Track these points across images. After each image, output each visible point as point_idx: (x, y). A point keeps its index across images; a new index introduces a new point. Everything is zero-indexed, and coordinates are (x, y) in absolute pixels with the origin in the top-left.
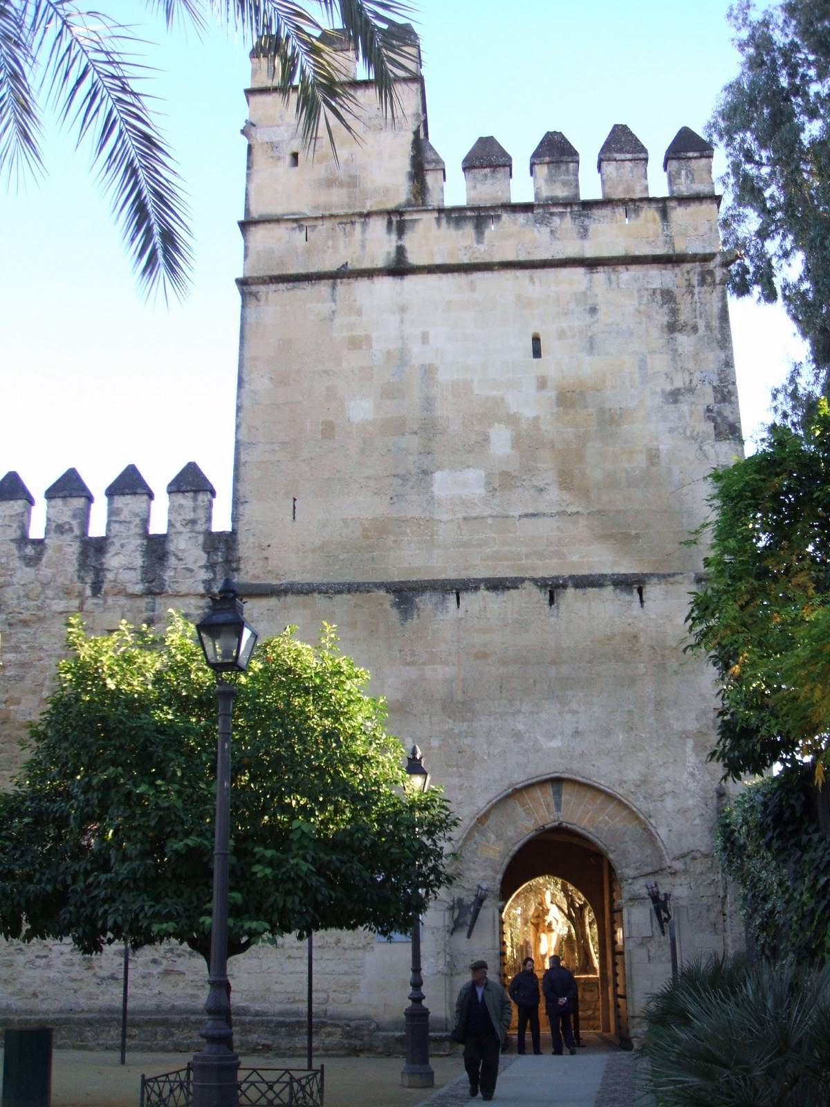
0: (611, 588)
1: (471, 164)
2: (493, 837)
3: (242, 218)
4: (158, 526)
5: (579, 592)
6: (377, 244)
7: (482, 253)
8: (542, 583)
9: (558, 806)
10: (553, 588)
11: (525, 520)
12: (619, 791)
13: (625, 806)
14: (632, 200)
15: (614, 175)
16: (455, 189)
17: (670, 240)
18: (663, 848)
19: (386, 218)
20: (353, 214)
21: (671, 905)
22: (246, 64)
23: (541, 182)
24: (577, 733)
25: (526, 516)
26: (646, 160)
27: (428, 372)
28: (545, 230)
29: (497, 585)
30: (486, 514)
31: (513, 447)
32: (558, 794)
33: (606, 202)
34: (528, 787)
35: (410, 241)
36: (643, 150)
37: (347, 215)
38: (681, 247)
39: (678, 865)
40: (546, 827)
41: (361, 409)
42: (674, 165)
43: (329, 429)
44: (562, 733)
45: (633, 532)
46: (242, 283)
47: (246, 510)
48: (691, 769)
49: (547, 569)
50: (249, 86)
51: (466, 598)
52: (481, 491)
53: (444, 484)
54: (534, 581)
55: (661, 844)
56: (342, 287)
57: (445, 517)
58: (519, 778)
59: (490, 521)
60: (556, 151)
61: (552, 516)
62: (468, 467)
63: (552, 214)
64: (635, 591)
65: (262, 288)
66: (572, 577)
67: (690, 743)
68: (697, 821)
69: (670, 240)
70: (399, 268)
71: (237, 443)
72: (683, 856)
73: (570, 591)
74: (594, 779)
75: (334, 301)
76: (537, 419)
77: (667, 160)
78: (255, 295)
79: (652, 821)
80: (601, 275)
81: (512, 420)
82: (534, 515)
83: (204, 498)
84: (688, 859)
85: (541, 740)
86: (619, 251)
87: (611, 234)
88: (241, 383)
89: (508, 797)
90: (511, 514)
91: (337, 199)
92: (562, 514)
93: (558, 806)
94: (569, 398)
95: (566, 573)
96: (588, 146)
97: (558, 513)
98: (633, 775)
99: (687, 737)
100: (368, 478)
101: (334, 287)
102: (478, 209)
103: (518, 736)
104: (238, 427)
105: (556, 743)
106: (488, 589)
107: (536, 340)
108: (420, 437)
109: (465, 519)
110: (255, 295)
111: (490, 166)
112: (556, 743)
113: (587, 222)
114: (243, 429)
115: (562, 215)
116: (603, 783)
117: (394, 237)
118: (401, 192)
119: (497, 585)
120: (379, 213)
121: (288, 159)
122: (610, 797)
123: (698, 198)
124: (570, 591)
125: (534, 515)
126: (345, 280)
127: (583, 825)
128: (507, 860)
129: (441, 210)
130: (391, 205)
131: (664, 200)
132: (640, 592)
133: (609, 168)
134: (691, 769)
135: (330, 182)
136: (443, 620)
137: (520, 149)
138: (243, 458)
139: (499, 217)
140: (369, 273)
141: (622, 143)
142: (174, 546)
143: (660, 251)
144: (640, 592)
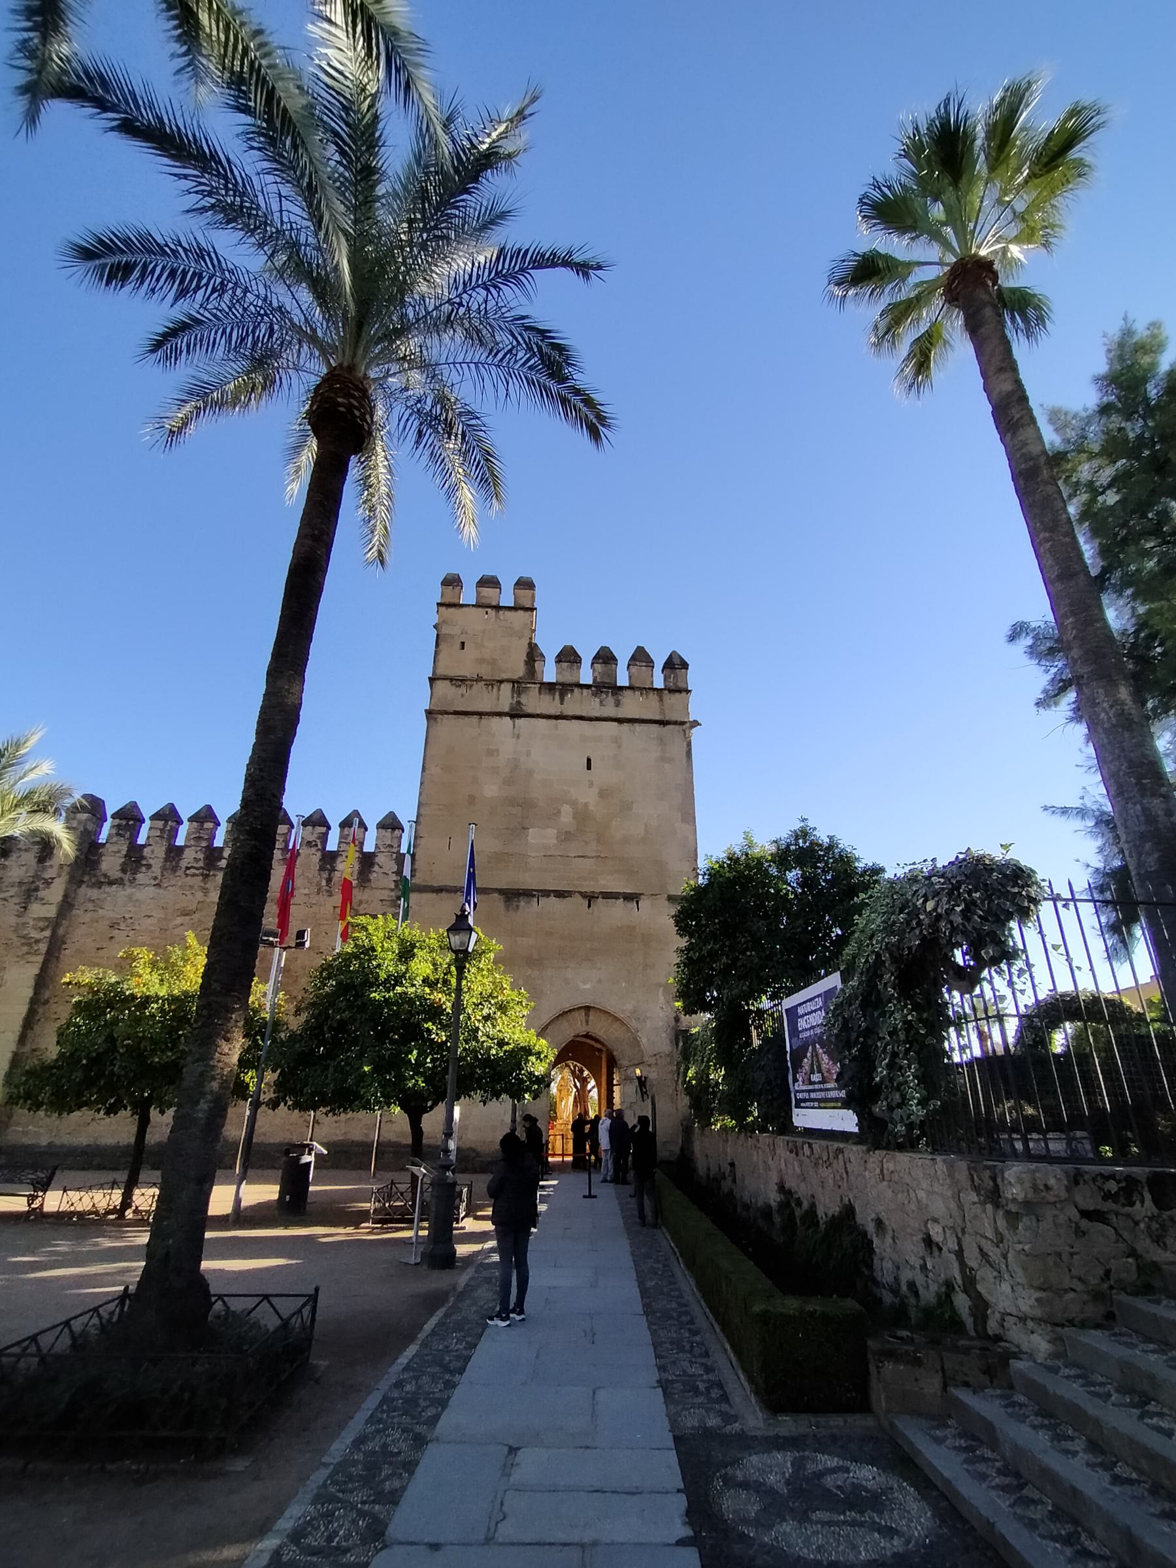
1: (560, 659)
4: (369, 847)
6: (504, 698)
8: (584, 895)
9: (587, 1021)
10: (590, 898)
12: (620, 1016)
16: (550, 673)
21: (648, 1084)
23: (596, 674)
24: (600, 981)
27: (530, 773)
28: (597, 700)
29: (560, 894)
32: (587, 1015)
33: (631, 688)
34: (570, 1011)
36: (652, 662)
39: (652, 1061)
41: (491, 790)
42: (667, 671)
43: (472, 799)
46: (429, 713)
47: (422, 842)
49: (588, 887)
51: (543, 900)
54: (580, 893)
56: (485, 721)
57: (533, 854)
58: (567, 1006)
60: (605, 657)
66: (601, 893)
67: (661, 989)
68: (664, 1035)
69: (662, 712)
70: (516, 714)
73: (600, 900)
77: (664, 668)
78: (435, 719)
81: (573, 803)
83: (397, 832)
87: (632, 706)
91: (485, 671)
93: (587, 1021)
94: (604, 794)
96: (623, 657)
98: (629, 1007)
102: (562, 684)
103: (567, 982)
104: (420, 794)
105: (588, 986)
107: (589, 760)
112: (588, 986)
116: (612, 1010)
118: (520, 671)
119: (560, 894)
120: (508, 681)
121: (459, 646)
122: (616, 1019)
123: (680, 691)
124: (600, 900)
129: (542, 684)
130: (516, 677)
133: (634, 669)
136: (531, 910)
137: (587, 656)
140: (500, 714)
141: (641, 657)
142: (380, 859)
143: (657, 718)
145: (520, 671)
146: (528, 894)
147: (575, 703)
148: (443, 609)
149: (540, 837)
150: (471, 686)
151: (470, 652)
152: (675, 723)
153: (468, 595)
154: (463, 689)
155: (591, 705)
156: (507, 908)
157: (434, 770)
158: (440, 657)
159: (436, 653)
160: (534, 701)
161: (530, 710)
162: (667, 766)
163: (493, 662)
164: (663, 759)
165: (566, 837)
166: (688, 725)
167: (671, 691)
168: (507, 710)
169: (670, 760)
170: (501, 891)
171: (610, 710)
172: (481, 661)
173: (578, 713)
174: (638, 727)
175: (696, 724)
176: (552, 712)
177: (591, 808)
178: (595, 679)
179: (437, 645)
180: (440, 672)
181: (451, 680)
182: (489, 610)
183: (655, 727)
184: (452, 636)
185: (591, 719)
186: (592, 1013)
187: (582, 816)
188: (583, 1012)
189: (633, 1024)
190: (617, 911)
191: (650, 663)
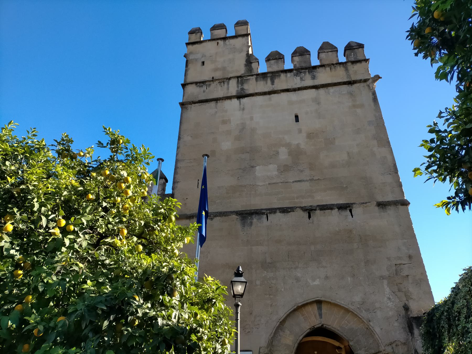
0: (337, 210)
2: (288, 332)
3: (183, 82)
5: (322, 212)
6: (233, 88)
8: (304, 209)
9: (321, 315)
10: (309, 211)
11: (295, 183)
12: (351, 307)
13: (356, 316)
14: (333, 64)
15: (325, 57)
17: (349, 76)
18: (379, 339)
19: (236, 79)
20: (224, 79)
22: (187, 36)
24: (327, 278)
25: (296, 181)
26: (337, 51)
28: (298, 78)
29: (284, 210)
30: (278, 182)
31: (289, 155)
32: (320, 309)
33: (322, 66)
35: (246, 86)
37: (221, 79)
38: (354, 78)
40: (315, 327)
41: (227, 145)
42: (347, 52)
44: (319, 278)
45: (345, 186)
46: (182, 105)
47: (179, 185)
48: (388, 296)
49: (307, 202)
50: (187, 42)
51: (271, 217)
52: (276, 173)
53: (260, 171)
55: (377, 337)
56: (220, 103)
57: (261, 184)
58: (300, 301)
59: (280, 184)
61: (307, 181)
62: (270, 164)
63: (301, 72)
64: (348, 211)
65: (190, 106)
66: (318, 206)
67: (385, 282)
68: (396, 324)
69: (349, 76)
71: (176, 160)
72: (391, 344)
73: (318, 212)
74: (338, 301)
75: (216, 108)
76: (298, 145)
78: (186, 108)
79: (371, 323)
80: (322, 91)
81: (288, 145)
82: (299, 181)
84: (394, 345)
85: (310, 281)
86: (329, 81)
87: (324, 77)
88: (179, 138)
89: (295, 310)
90: (290, 181)
91: (218, 75)
92: (311, 180)
93: (321, 315)
94: (310, 136)
95: (315, 204)
97: (310, 180)
98: (357, 298)
99: (383, 279)
100: (229, 170)
101: (217, 102)
102: (272, 73)
103: (298, 280)
104: (177, 154)
105: (317, 282)
106: (280, 212)
107: (297, 117)
108: (249, 155)
109: (269, 184)
110: (186, 108)
111: (276, 59)
112: (317, 282)
113: (315, 73)
114: (180, 155)
115: (305, 73)
116: (342, 303)
117: (240, 85)
118: (242, 70)
119: (284, 210)
121: (200, 63)
122: (347, 311)
123: (360, 61)
124: (318, 212)
125: (299, 181)
126: (221, 101)
127: (334, 326)
128: (296, 345)
129: (258, 75)
130: (239, 74)
131: (346, 63)
132: (351, 211)
133: (323, 55)
134: (388, 296)
136: (260, 225)
138: (179, 165)
139: (280, 75)
140: (230, 98)
143: (345, 80)
144: (351, 211)
145: (242, 70)
146: (258, 213)
147: (282, 82)
148: (190, 47)
149: (265, 172)
150: (210, 85)
151: (209, 66)
152: (360, 81)
153: (205, 36)
154: (204, 88)
155: (295, 82)
156: (244, 225)
157: (187, 138)
158: (189, 72)
159: (186, 71)
160: (252, 86)
161: (251, 92)
162: (359, 111)
163: (224, 69)
164: (354, 106)
165: (285, 169)
166: (370, 81)
167: (353, 62)
168: (234, 93)
169: (362, 106)
170: (239, 213)
171: (309, 82)
172: (216, 70)
173: (285, 87)
174: (332, 90)
175: (377, 78)
176: (266, 90)
177: (302, 146)
178: (295, 66)
179: (187, 66)
180: (189, 80)
181: (196, 83)
182: (219, 41)
183: (345, 88)
184: (196, 60)
185: (294, 90)
186: (324, 308)
187: (296, 154)
188: (315, 307)
189: (364, 314)
190: (334, 219)
191: (334, 49)
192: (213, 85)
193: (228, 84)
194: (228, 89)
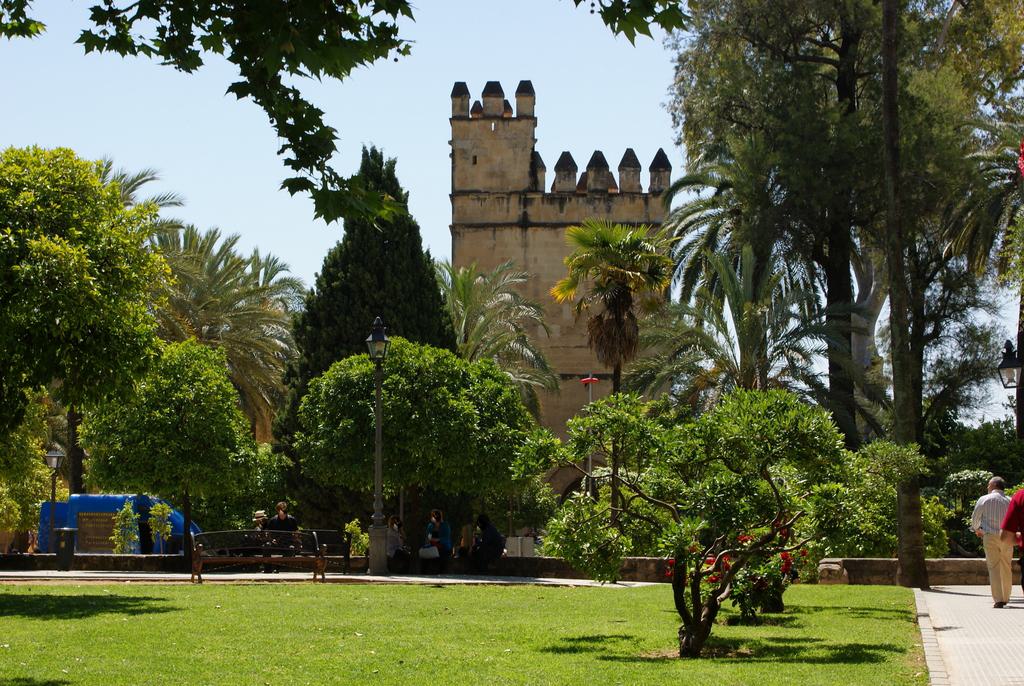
6: (514, 211)
7: (563, 217)
17: (647, 216)
28: (591, 207)
35: (531, 210)
70: (524, 224)
75: (495, 239)
91: (494, 183)
117: (522, 207)
121: (471, 160)
135: (491, 175)
151: (483, 167)
192: (490, 199)
193: (508, 202)
194: (508, 211)
